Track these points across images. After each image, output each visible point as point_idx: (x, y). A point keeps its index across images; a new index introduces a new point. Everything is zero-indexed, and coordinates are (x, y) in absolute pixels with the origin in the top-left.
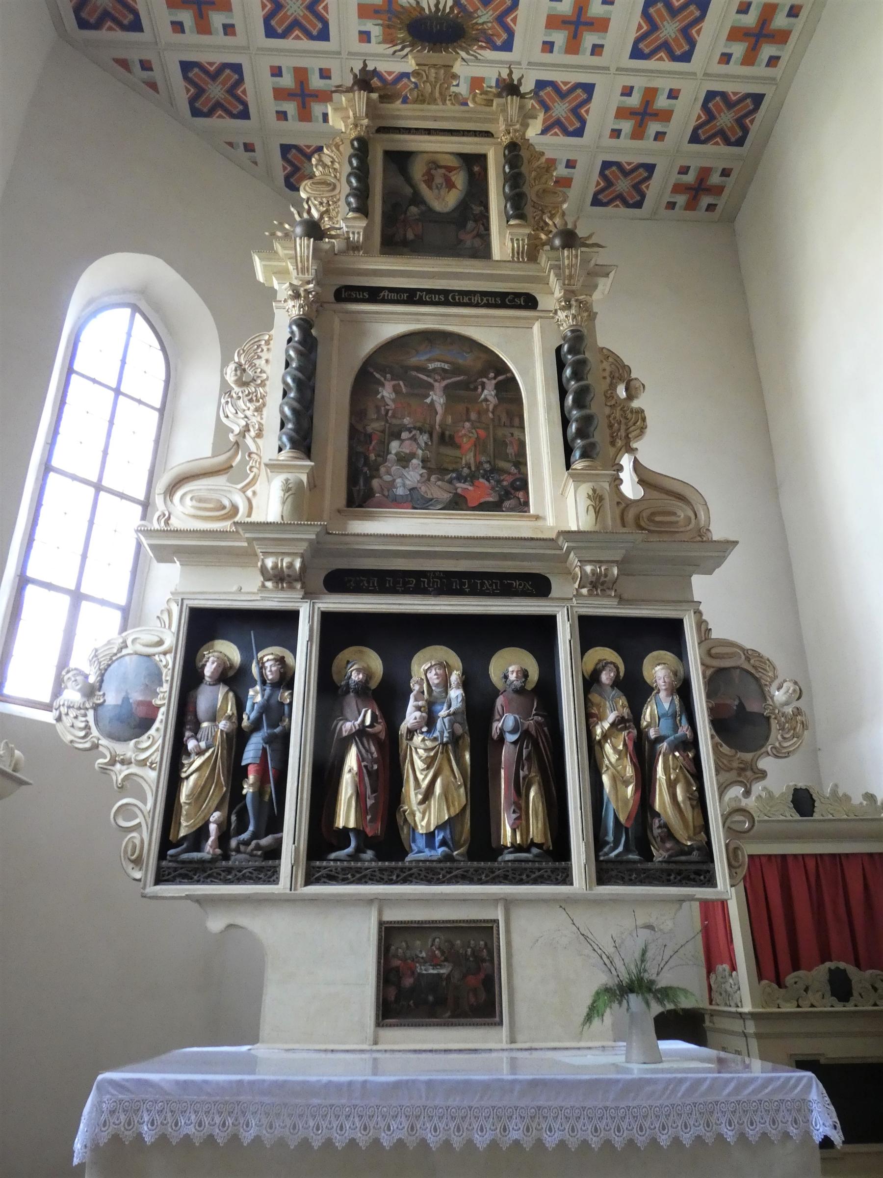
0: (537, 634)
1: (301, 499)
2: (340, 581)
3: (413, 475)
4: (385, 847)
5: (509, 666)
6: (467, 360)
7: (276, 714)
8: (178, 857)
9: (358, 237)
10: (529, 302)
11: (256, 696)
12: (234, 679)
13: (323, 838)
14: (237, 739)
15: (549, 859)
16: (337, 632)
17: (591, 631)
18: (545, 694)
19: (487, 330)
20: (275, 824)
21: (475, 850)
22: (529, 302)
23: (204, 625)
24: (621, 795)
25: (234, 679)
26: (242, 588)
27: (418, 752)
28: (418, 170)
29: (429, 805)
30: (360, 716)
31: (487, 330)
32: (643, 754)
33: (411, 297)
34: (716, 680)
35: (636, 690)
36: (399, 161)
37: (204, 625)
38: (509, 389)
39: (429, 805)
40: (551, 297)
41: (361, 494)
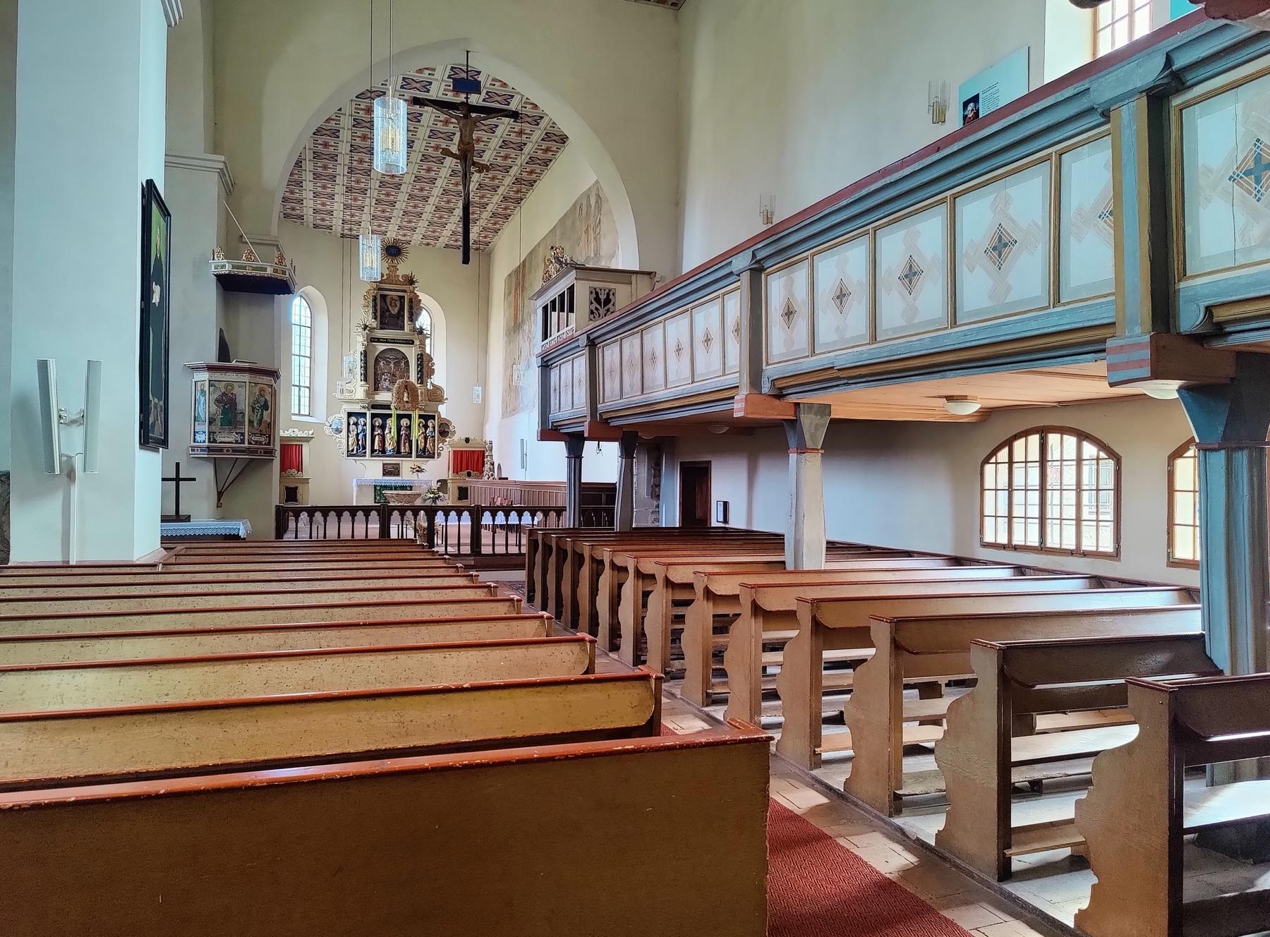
0: (409, 417)
1: (368, 394)
2: (374, 407)
3: (387, 383)
4: (383, 451)
5: (404, 422)
6: (400, 356)
7: (364, 430)
8: (350, 454)
9: (374, 325)
10: (412, 343)
11: (360, 428)
12: (356, 424)
13: (373, 451)
14: (357, 435)
15: (409, 454)
16: (373, 416)
17: (420, 416)
18: (409, 427)
19: (403, 348)
20: (364, 448)
21: (398, 452)
22: (412, 343)
23: (350, 415)
24: (421, 446)
25: (356, 424)
26: (357, 408)
27: (388, 437)
28: (388, 301)
29: (389, 447)
30: (378, 431)
31: (403, 348)
32: (426, 438)
33: (387, 341)
34: (441, 425)
35: (426, 427)
36: (384, 297)
37: (350, 415)
38: (407, 363)
39: (389, 447)
40: (417, 342)
41: (376, 389)
